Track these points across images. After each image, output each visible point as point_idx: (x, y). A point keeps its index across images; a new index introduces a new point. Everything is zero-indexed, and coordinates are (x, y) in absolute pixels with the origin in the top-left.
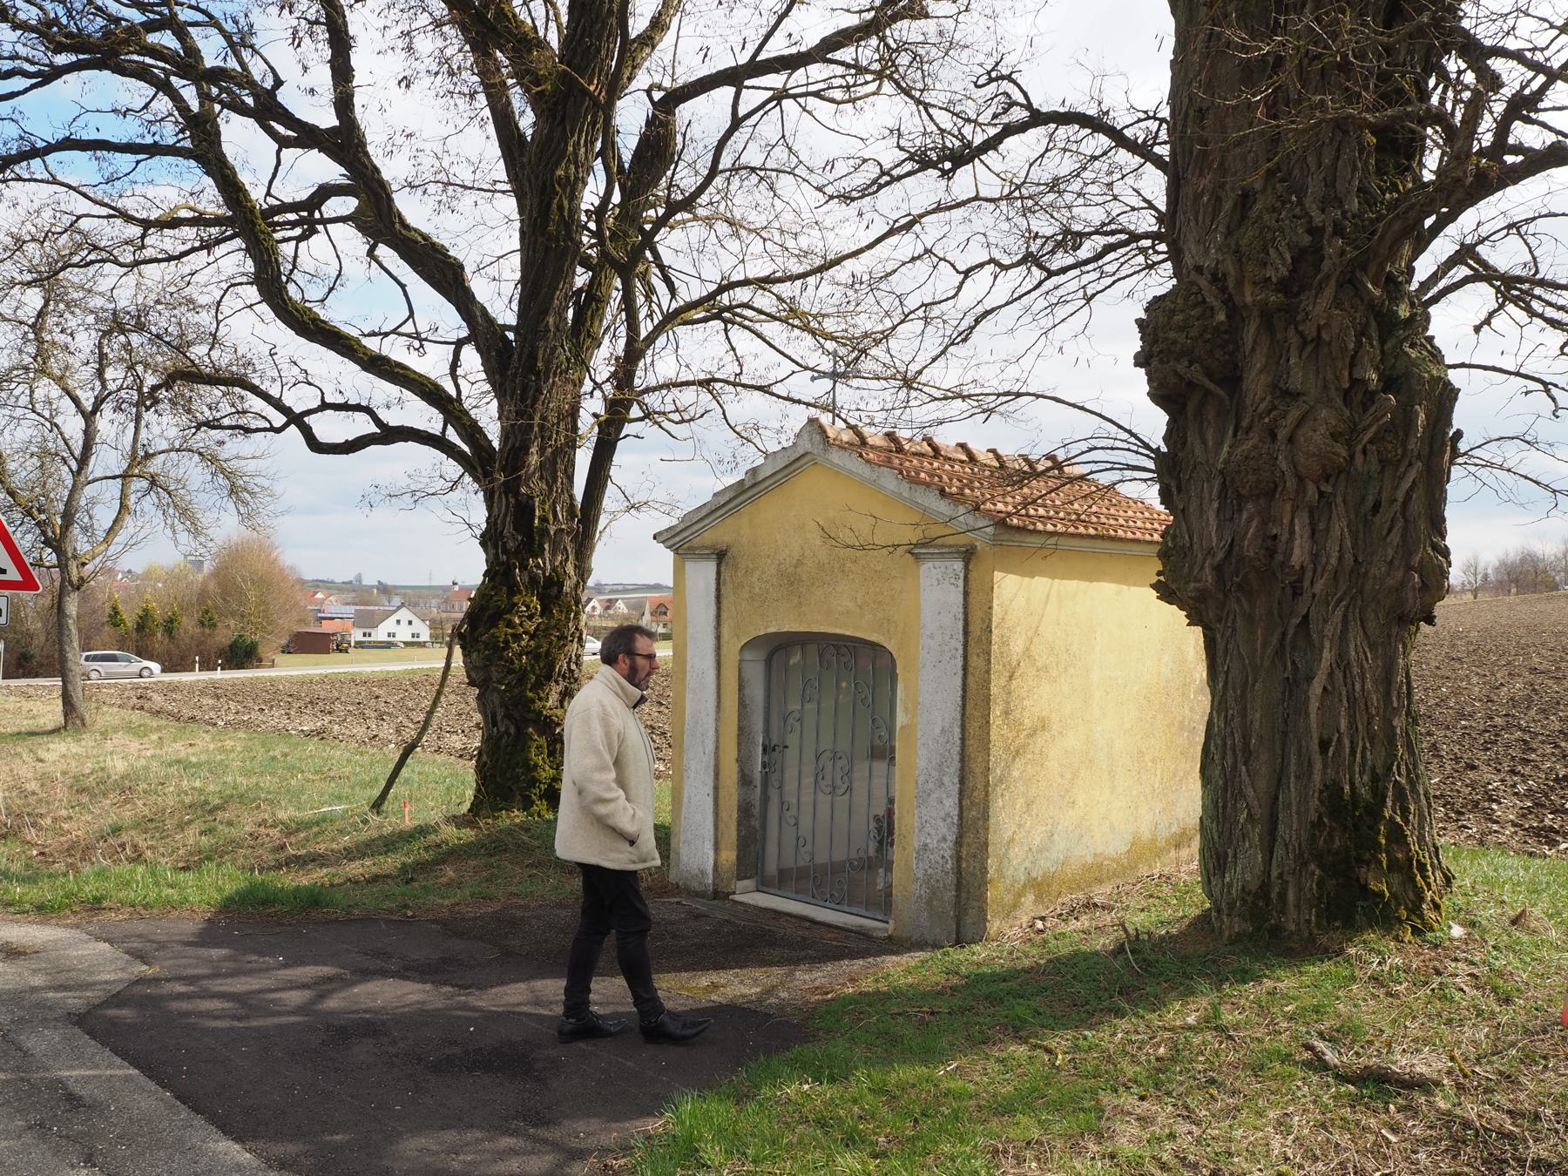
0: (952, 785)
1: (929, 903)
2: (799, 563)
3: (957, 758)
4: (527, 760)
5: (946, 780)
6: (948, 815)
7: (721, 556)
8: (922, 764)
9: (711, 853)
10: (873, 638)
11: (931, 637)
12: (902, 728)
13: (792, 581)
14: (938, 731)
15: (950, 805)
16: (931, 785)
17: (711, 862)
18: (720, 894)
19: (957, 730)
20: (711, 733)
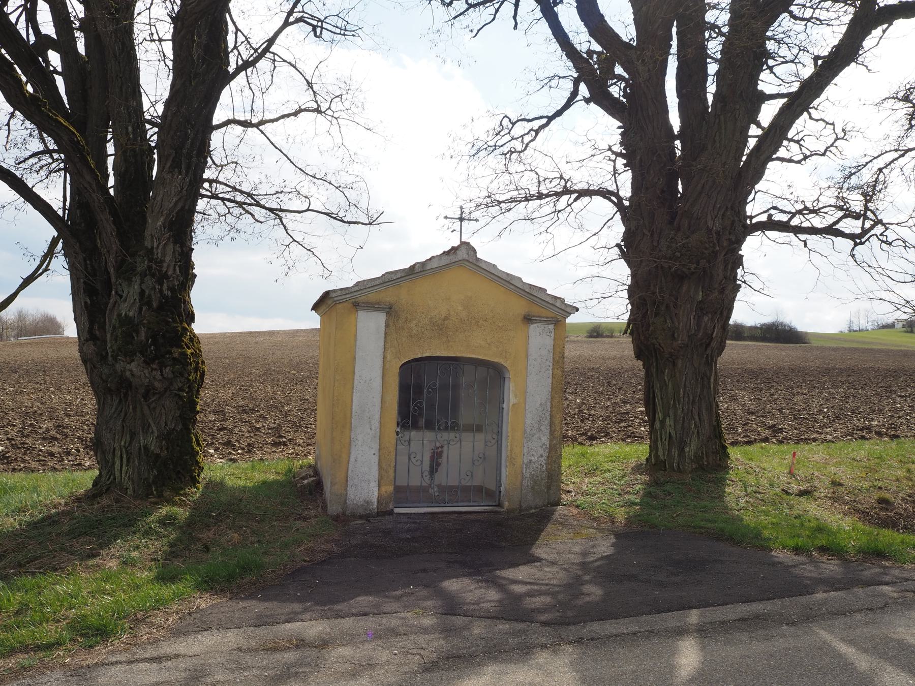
0: (546, 429)
1: (533, 488)
2: (446, 319)
3: (548, 417)
4: (193, 449)
5: (542, 428)
6: (544, 444)
7: (390, 311)
8: (528, 421)
9: (376, 489)
10: (496, 360)
11: (535, 360)
12: (513, 405)
13: (441, 327)
14: (538, 405)
15: (545, 439)
16: (534, 431)
17: (376, 494)
18: (384, 513)
19: (549, 404)
20: (377, 417)
